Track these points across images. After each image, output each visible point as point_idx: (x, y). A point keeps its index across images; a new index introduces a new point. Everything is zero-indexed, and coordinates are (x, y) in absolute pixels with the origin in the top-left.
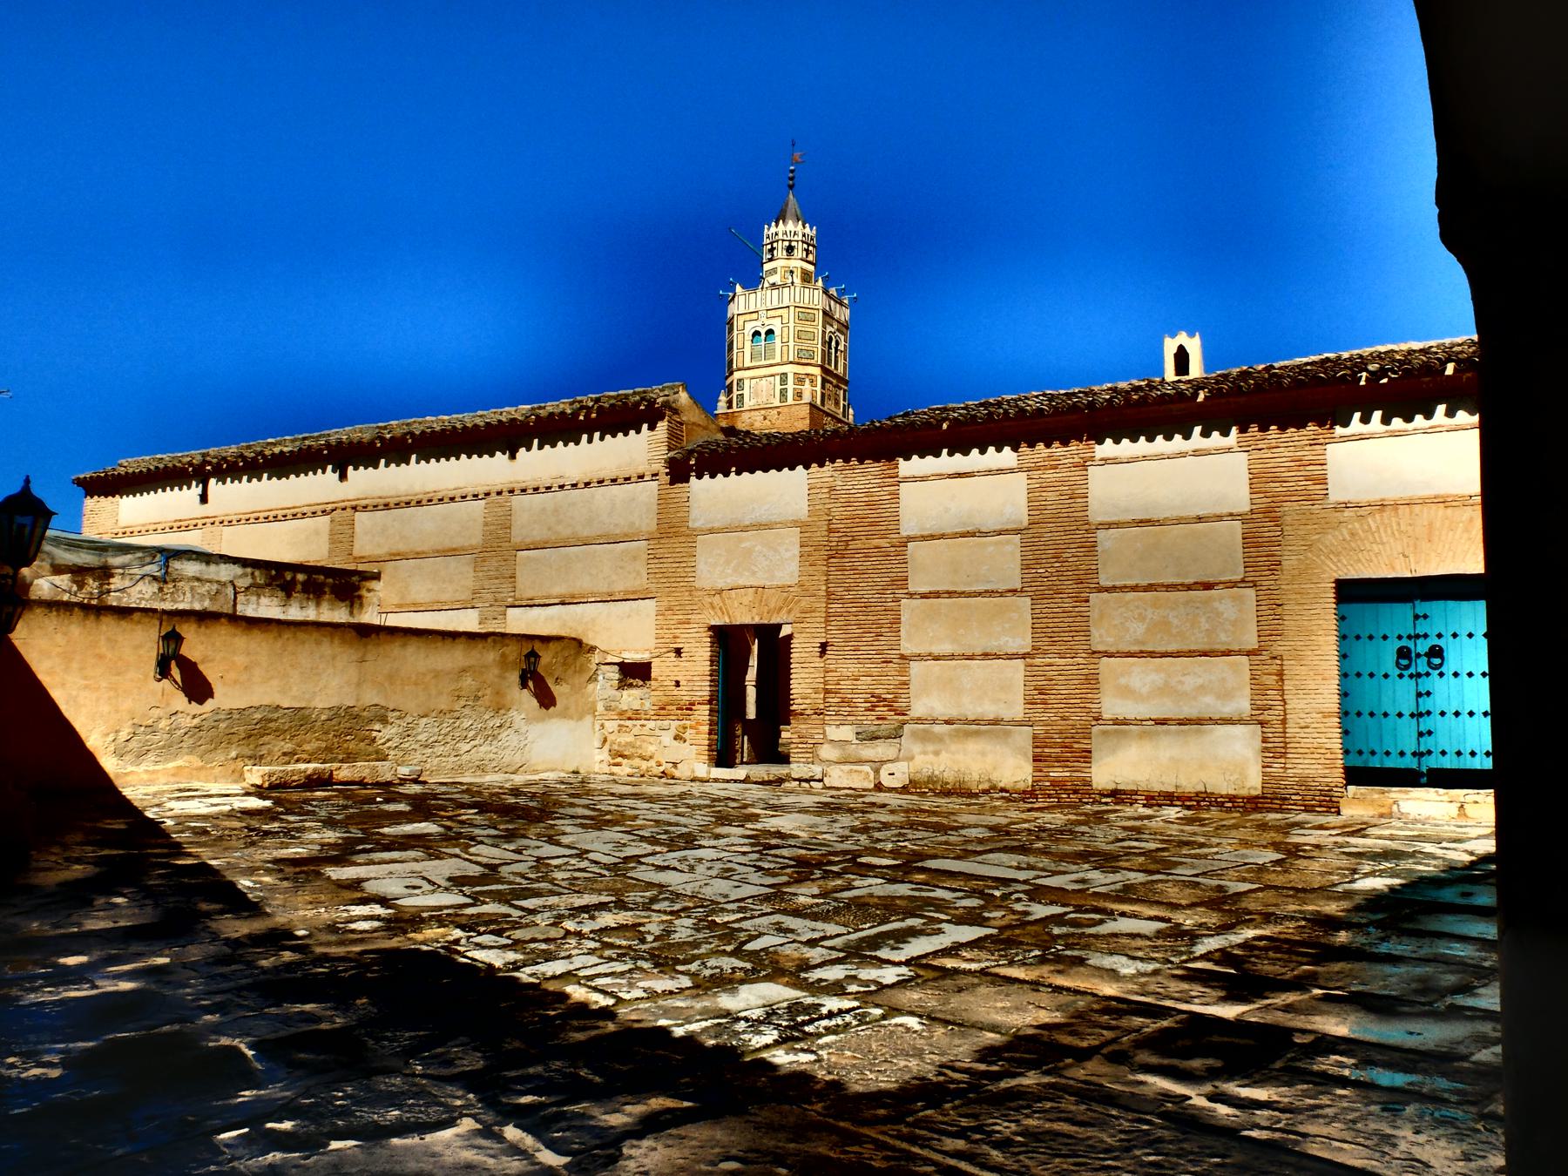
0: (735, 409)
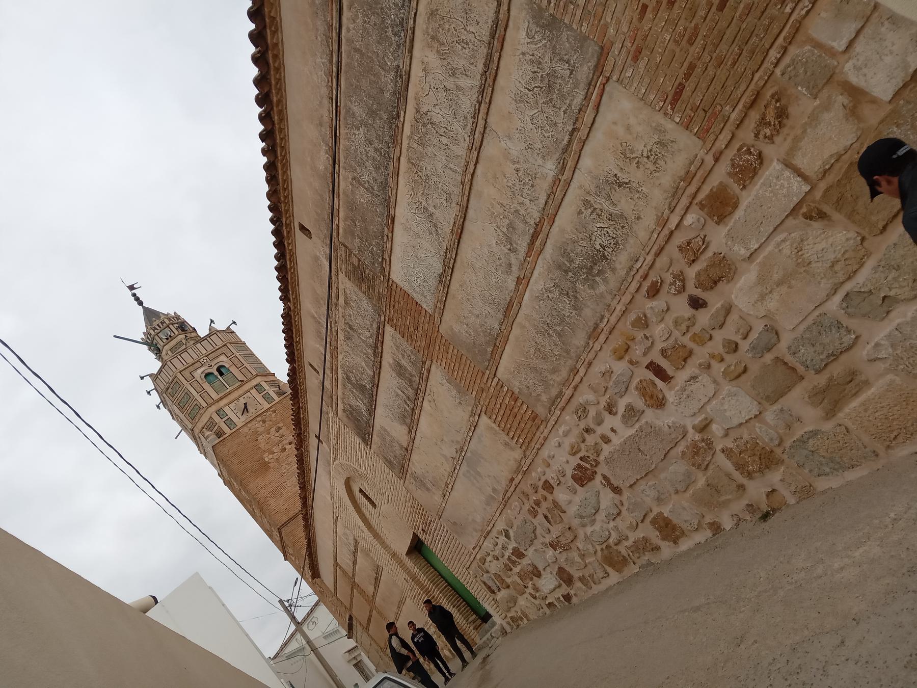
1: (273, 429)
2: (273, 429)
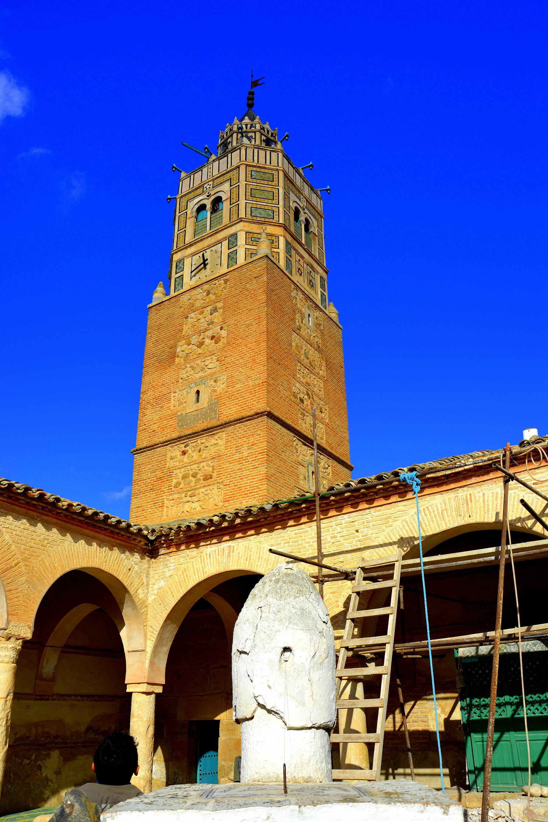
0: (172, 294)
1: (209, 308)
2: (209, 308)
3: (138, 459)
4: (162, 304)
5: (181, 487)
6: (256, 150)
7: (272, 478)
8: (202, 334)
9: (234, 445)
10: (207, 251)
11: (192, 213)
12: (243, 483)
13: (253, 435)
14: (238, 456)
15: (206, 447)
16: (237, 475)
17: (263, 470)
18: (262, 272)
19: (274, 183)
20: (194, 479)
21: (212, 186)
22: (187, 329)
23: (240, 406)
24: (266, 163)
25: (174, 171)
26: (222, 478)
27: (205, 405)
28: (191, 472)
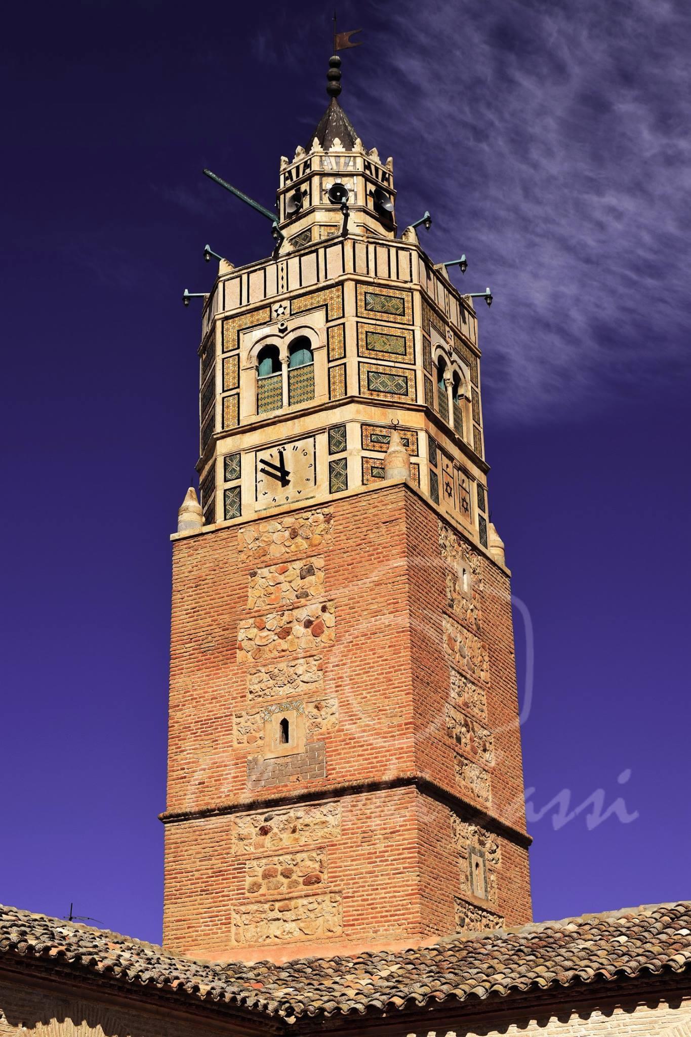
2: (298, 565)
3: (173, 831)
4: (200, 538)
5: (261, 891)
6: (371, 248)
7: (427, 890)
8: (286, 613)
9: (358, 828)
10: (286, 446)
11: (249, 357)
12: (378, 897)
13: (392, 814)
14: (366, 848)
15: (307, 825)
16: (366, 882)
17: (412, 878)
18: (397, 513)
19: (405, 319)
20: (286, 881)
21: (287, 311)
22: (255, 598)
23: (366, 759)
24: (390, 277)
25: (208, 261)
26: (339, 885)
27: (302, 750)
28: (280, 868)
